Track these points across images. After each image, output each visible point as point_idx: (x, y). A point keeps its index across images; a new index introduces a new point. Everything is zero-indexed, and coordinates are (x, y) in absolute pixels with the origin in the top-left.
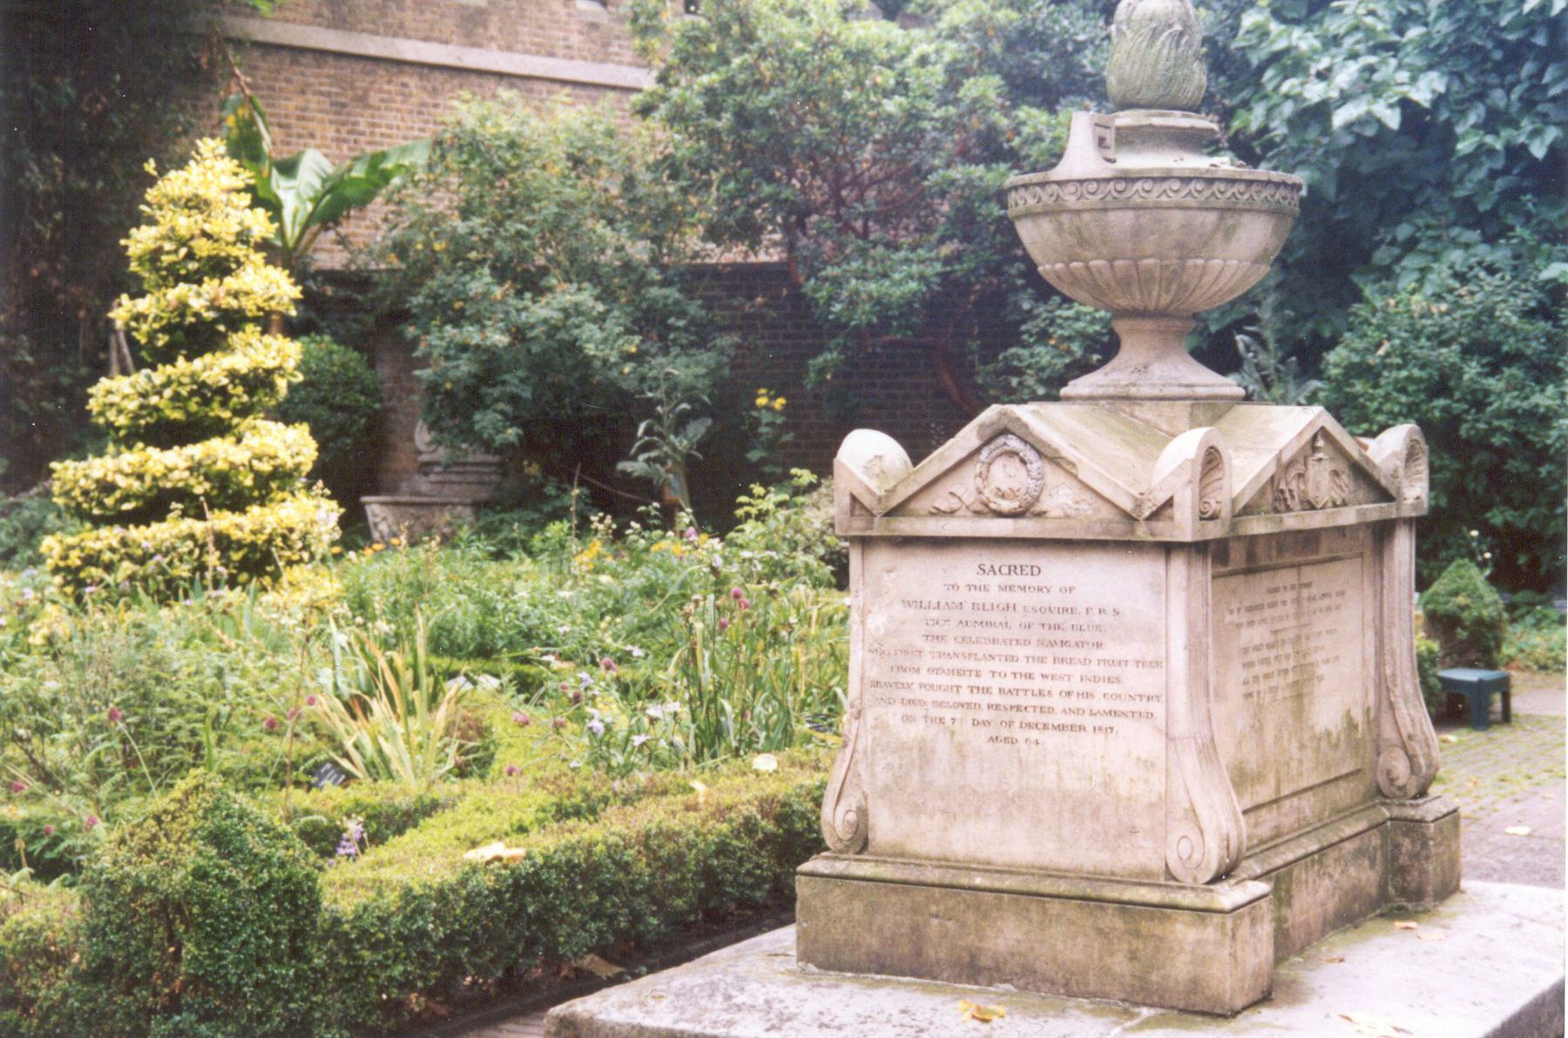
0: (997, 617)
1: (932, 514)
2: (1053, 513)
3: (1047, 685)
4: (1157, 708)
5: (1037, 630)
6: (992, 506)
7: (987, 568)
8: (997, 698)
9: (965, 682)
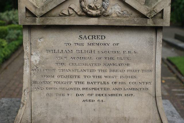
0: (87, 55)
1: (60, 16)
2: (114, 15)
3: (108, 80)
4: (148, 86)
5: (103, 61)
6: (89, 13)
7: (83, 37)
8: (86, 86)
9: (73, 80)
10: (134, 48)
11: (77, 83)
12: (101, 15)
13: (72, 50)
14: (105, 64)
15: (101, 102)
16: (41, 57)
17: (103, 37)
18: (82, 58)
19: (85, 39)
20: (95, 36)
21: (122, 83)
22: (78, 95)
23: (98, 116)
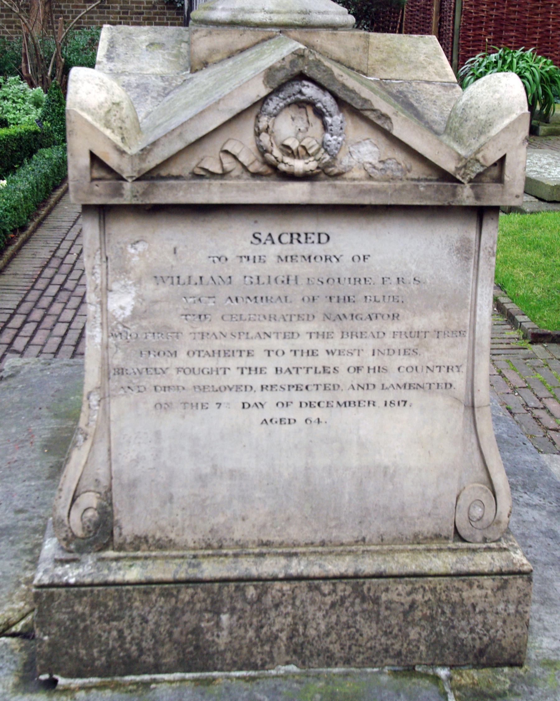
0: (274, 291)
1: (196, 176)
2: (357, 173)
5: (322, 305)
6: (282, 167)
7: (264, 237)
8: (270, 378)
9: (233, 363)
10: (414, 268)
11: (246, 372)
12: (318, 174)
13: (230, 277)
14: (329, 316)
15: (315, 425)
16: (139, 297)
17: (324, 238)
18: (259, 299)
19: (269, 243)
20: (299, 235)
21: (377, 369)
22: (246, 406)
23: (307, 463)
